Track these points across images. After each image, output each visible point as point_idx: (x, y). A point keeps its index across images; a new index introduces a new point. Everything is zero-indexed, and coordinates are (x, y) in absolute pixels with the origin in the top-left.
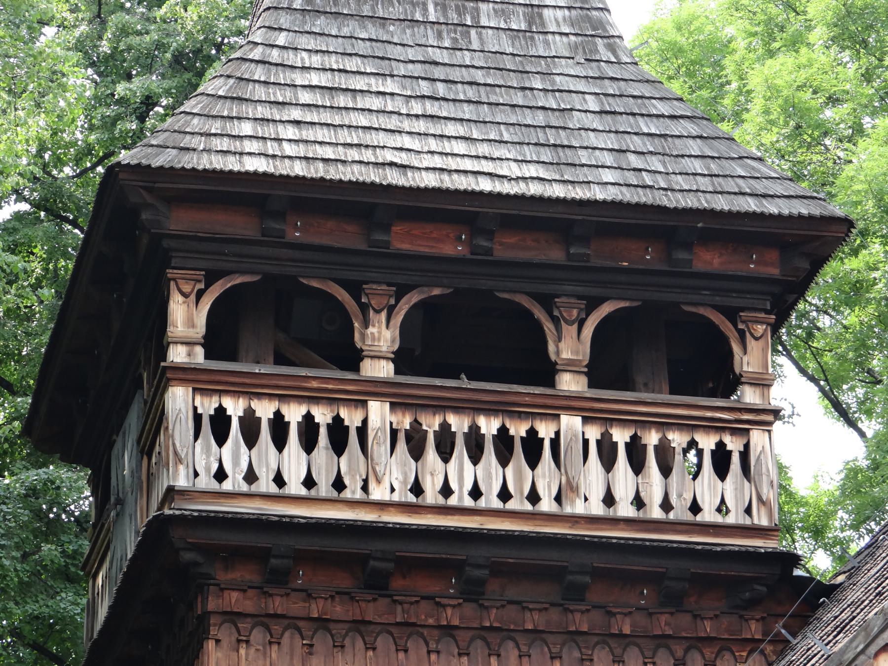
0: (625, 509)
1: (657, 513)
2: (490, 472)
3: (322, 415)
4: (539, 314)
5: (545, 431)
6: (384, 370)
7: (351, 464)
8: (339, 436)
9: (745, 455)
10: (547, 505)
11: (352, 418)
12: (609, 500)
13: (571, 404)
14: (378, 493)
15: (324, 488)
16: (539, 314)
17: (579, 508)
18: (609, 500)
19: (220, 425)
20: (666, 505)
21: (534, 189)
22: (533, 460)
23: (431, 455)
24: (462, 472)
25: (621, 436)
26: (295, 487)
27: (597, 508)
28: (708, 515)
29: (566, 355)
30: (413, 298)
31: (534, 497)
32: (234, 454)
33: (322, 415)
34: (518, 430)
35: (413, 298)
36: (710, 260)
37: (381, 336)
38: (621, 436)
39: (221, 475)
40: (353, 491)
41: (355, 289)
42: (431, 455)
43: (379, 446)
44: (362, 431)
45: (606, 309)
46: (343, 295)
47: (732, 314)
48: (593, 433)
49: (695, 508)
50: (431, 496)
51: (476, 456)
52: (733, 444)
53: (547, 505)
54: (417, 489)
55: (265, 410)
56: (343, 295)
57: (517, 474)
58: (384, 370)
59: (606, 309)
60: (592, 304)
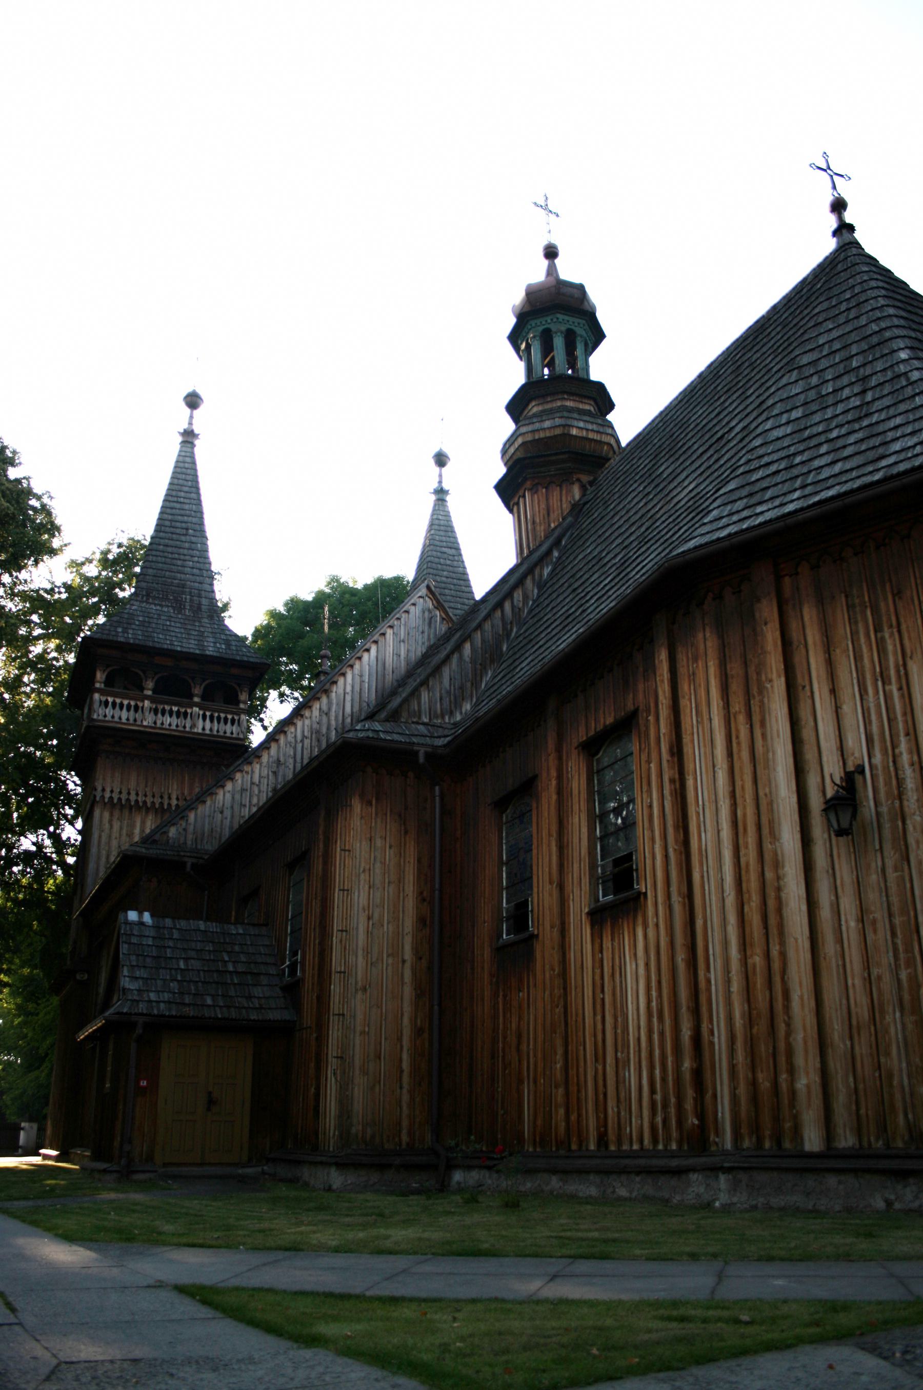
0: (208, 732)
1: (215, 733)
2: (174, 721)
3: (133, 703)
4: (190, 681)
5: (189, 711)
6: (149, 693)
7: (139, 715)
8: (136, 708)
9: (239, 720)
10: (188, 729)
11: (140, 704)
12: (204, 729)
13: (196, 705)
14: (145, 723)
15: (131, 721)
16: (190, 681)
17: (196, 730)
18: (204, 729)
19: (106, 704)
20: (218, 731)
21: (192, 651)
22: (185, 718)
23: (160, 715)
24: (168, 720)
25: (208, 714)
26: (124, 720)
27: (200, 731)
28: (228, 734)
29: (196, 692)
30: (159, 675)
31: (185, 727)
32: (109, 711)
33: (133, 703)
34: (183, 710)
35: (159, 675)
36: (235, 671)
37: (150, 684)
38: (208, 714)
39: (105, 716)
40: (139, 723)
41: (144, 672)
42: (160, 715)
43: (147, 713)
44: (143, 708)
45: (207, 682)
46: (141, 673)
47: (239, 685)
48: (201, 712)
49: (225, 733)
50: (158, 725)
51: (171, 716)
52: (236, 718)
53: (188, 729)
54: (155, 723)
55: (118, 701)
56: (141, 673)
57: (181, 721)
58: (149, 693)
59: (207, 682)
60: (204, 680)
